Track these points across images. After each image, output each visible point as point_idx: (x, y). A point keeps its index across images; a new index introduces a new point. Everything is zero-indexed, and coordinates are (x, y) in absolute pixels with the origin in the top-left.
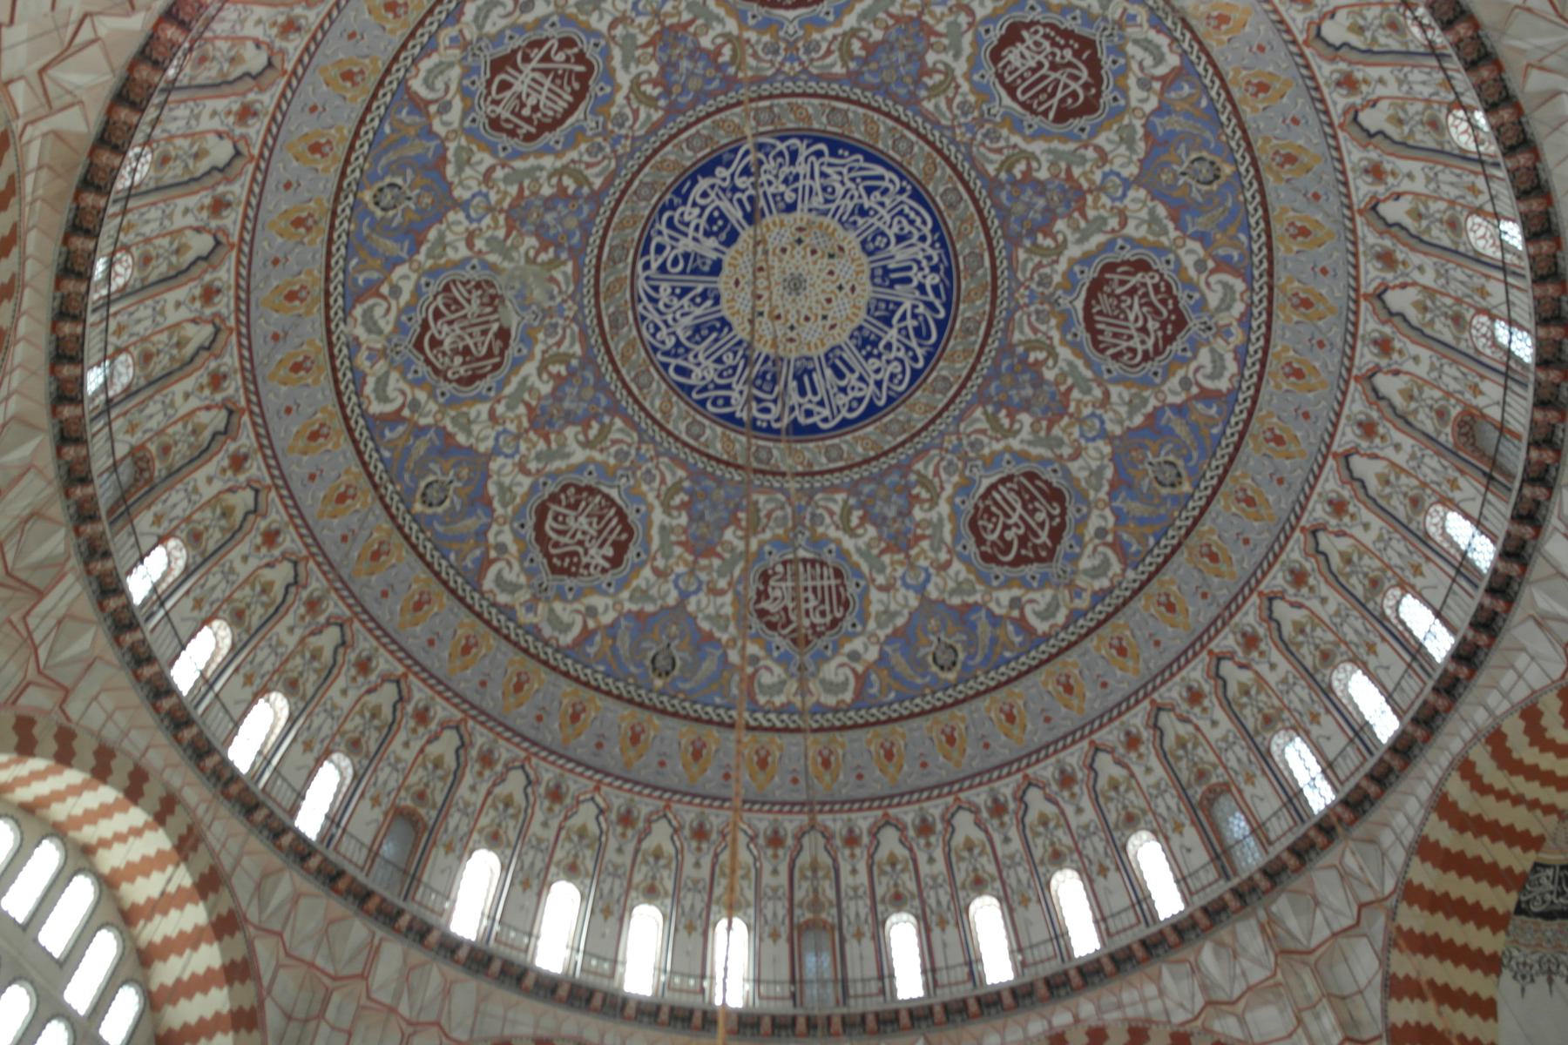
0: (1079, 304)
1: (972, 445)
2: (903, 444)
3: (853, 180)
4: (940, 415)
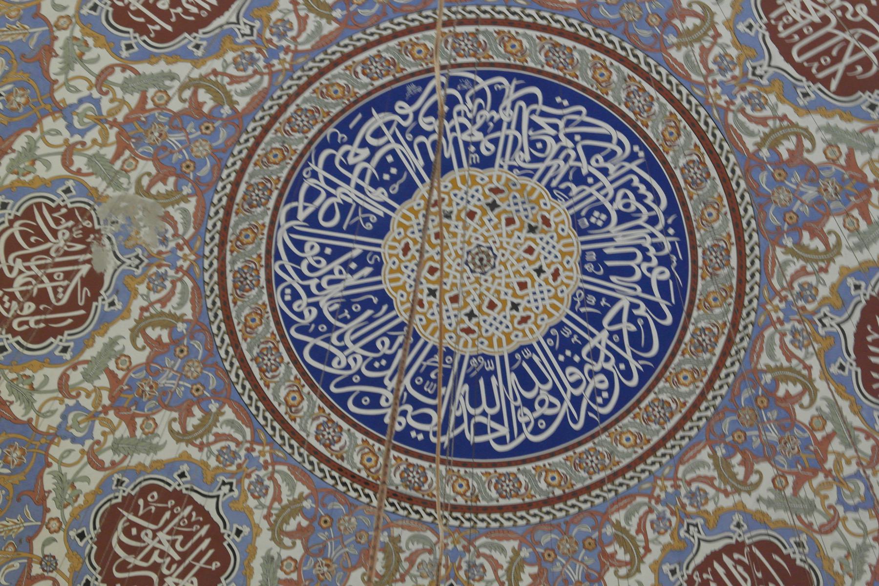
0: (850, 328)
1: (692, 496)
2: (600, 484)
3: (570, 136)
4: (653, 451)
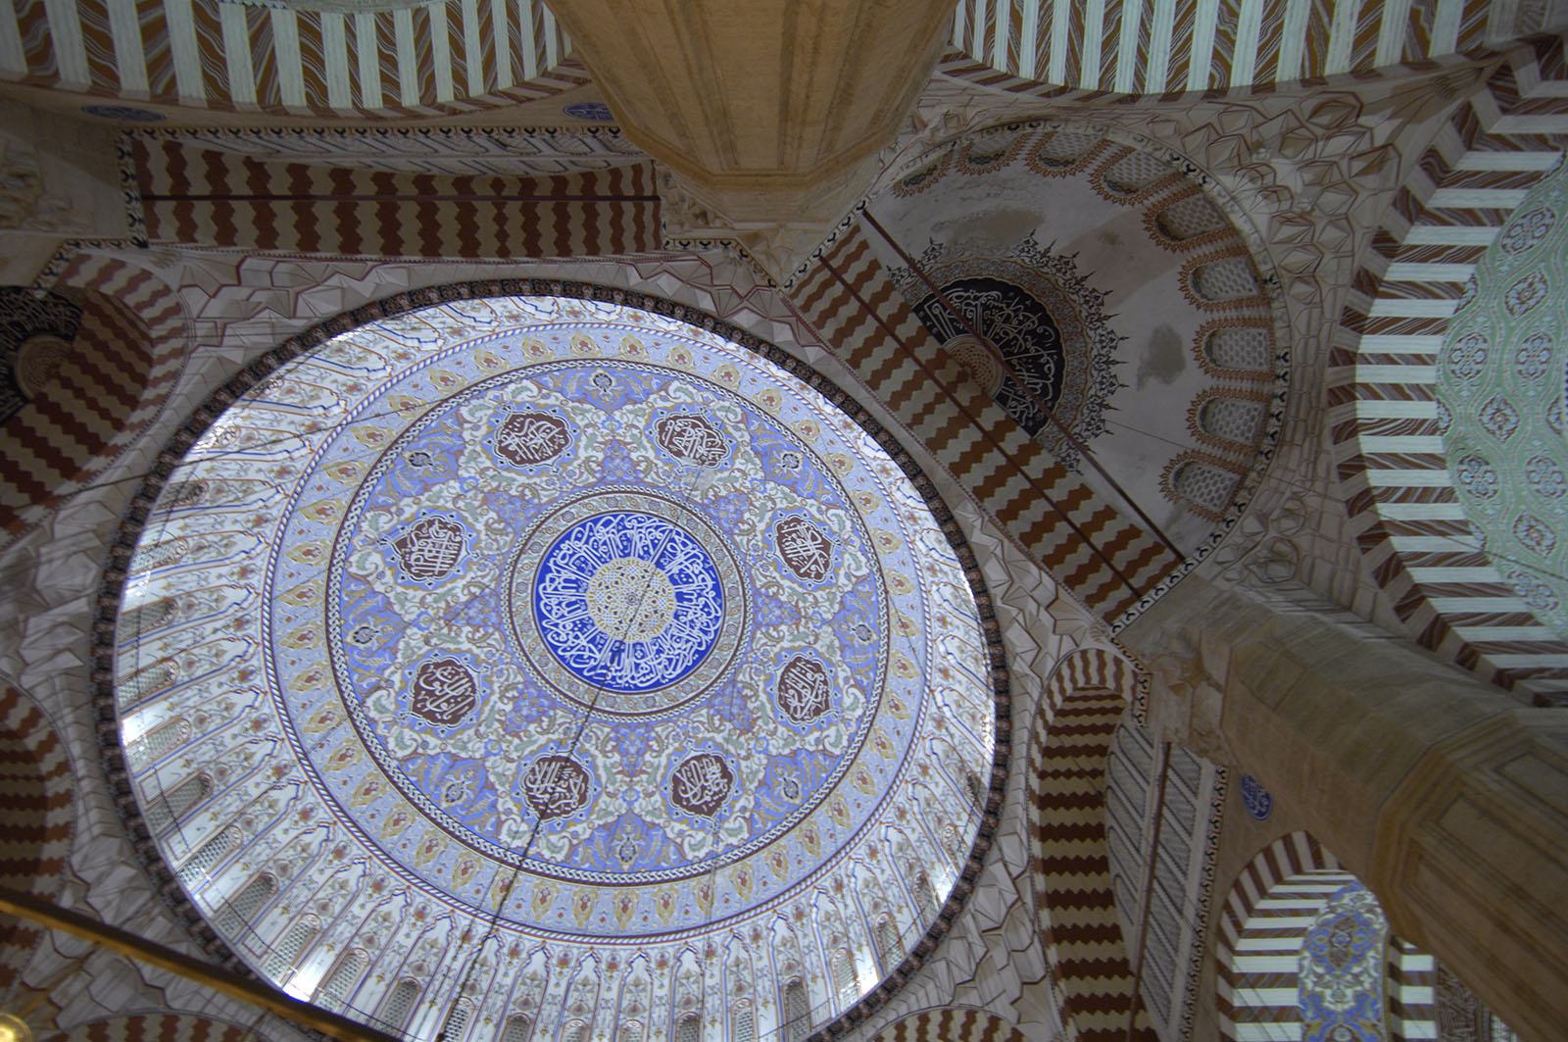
1: (501, 671)
2: (514, 629)
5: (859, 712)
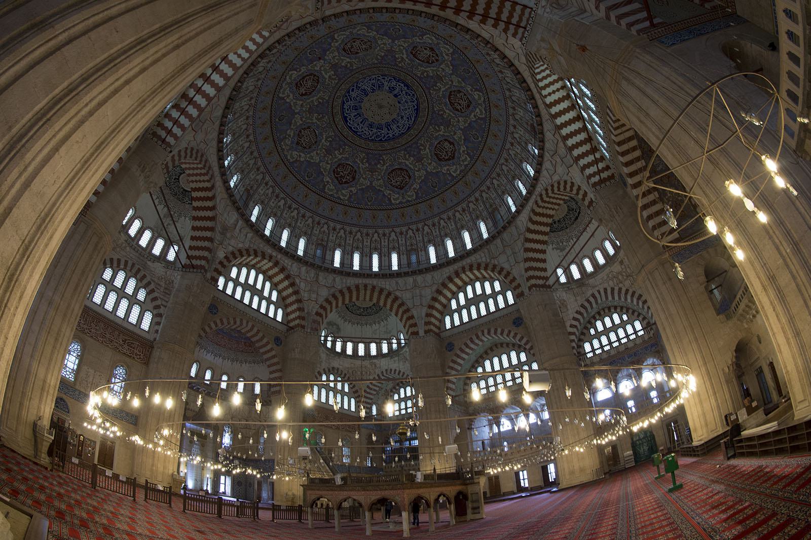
5: (482, 99)
